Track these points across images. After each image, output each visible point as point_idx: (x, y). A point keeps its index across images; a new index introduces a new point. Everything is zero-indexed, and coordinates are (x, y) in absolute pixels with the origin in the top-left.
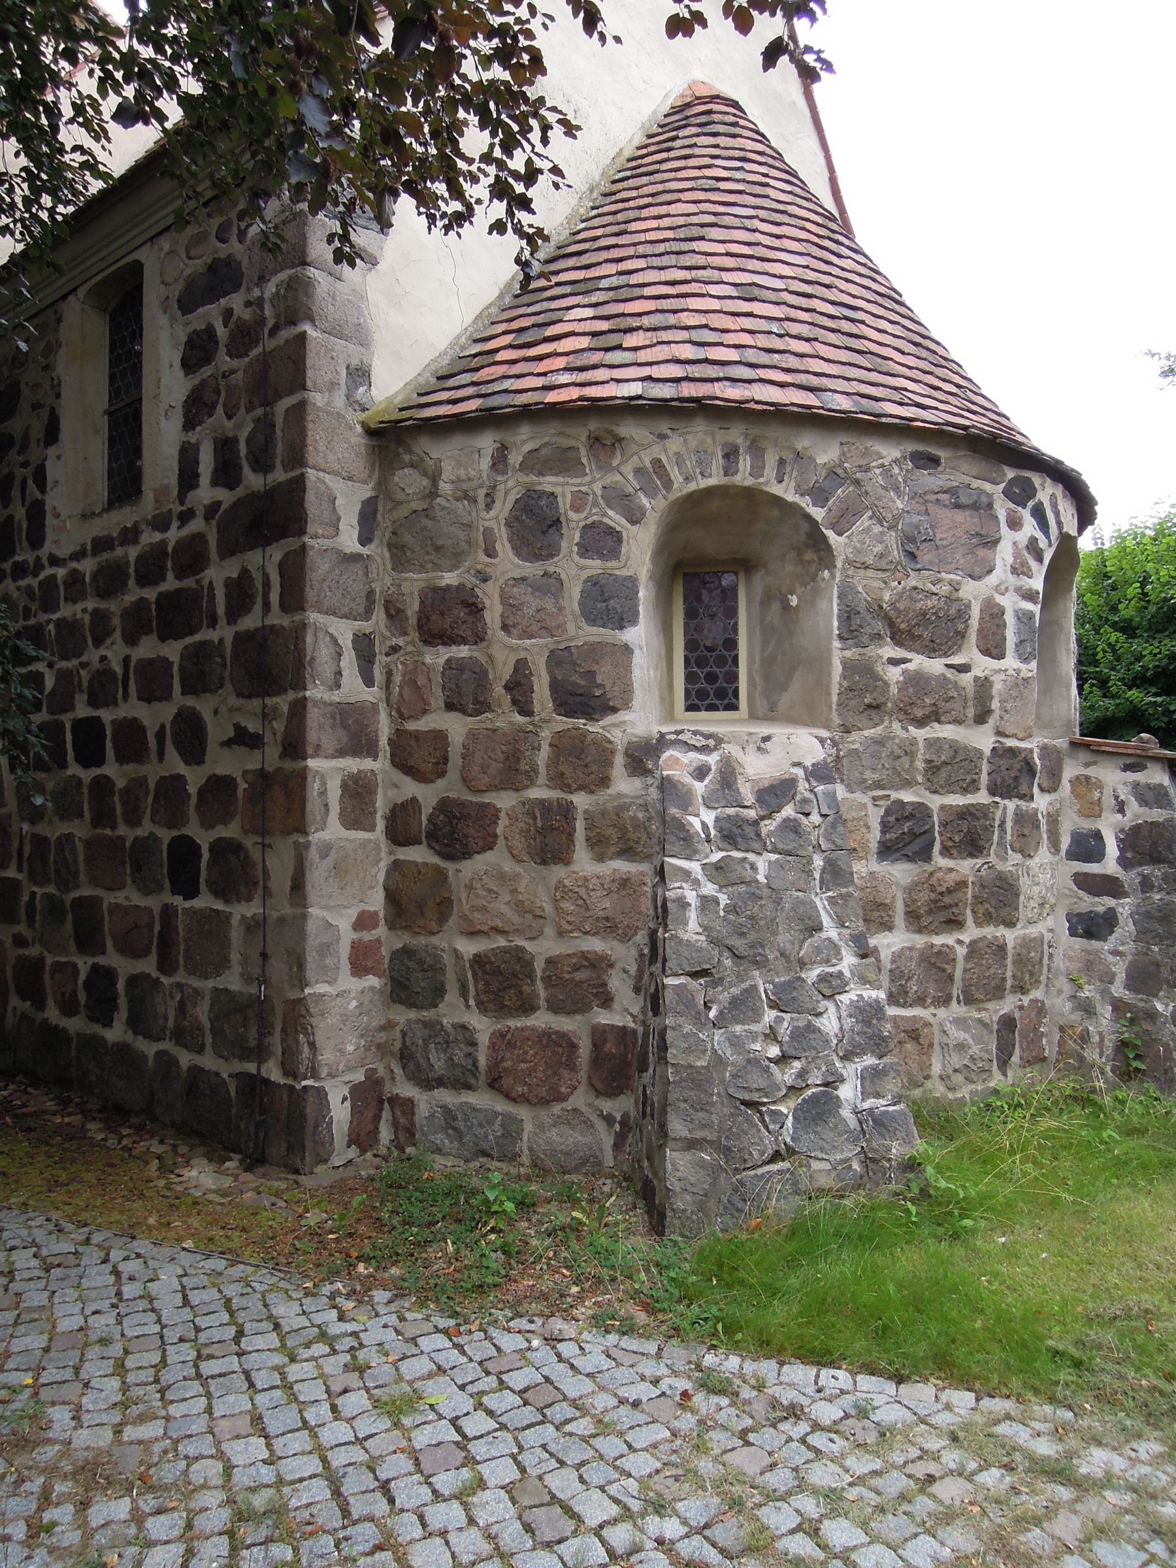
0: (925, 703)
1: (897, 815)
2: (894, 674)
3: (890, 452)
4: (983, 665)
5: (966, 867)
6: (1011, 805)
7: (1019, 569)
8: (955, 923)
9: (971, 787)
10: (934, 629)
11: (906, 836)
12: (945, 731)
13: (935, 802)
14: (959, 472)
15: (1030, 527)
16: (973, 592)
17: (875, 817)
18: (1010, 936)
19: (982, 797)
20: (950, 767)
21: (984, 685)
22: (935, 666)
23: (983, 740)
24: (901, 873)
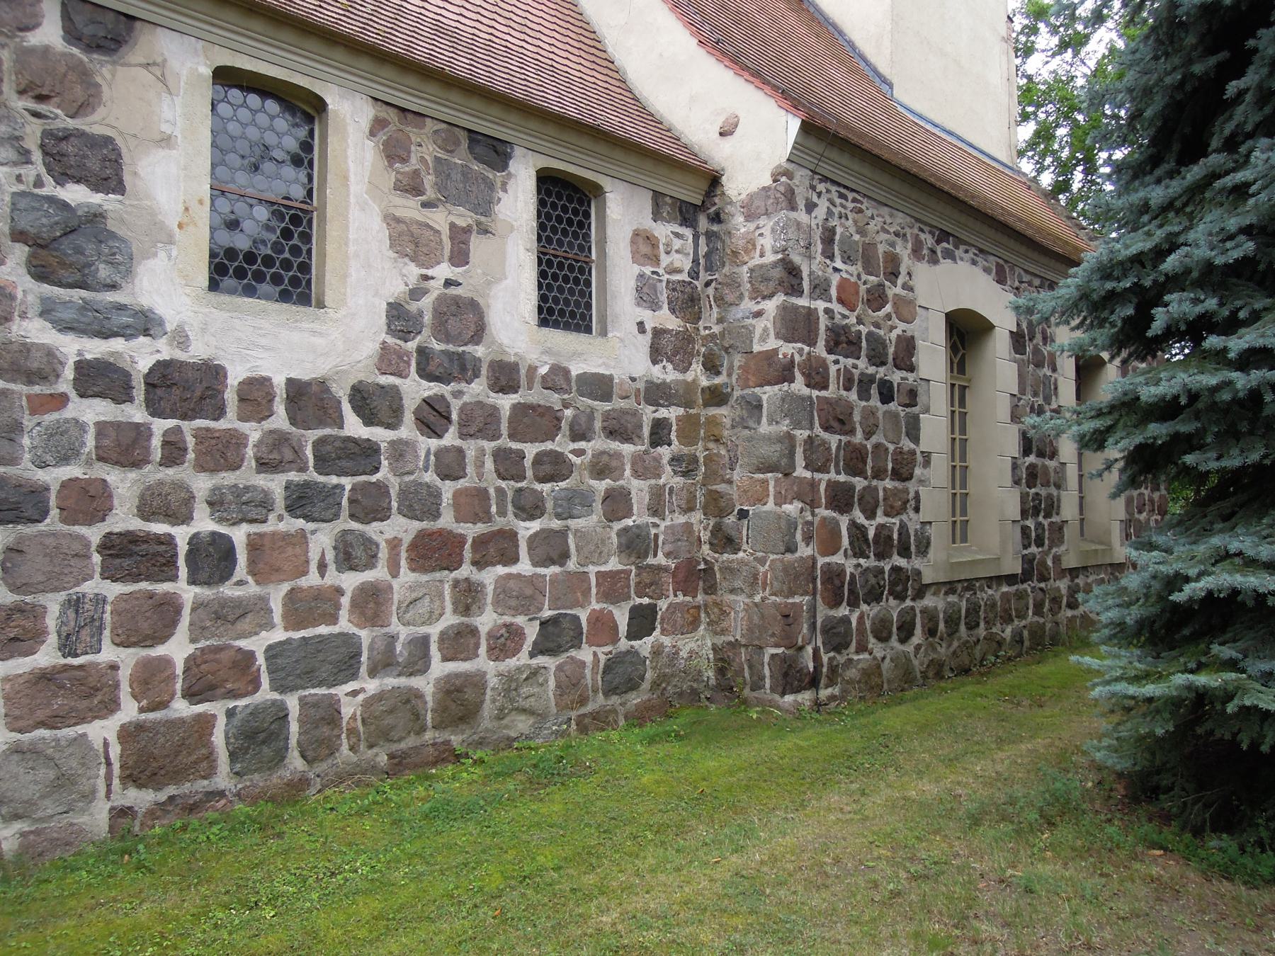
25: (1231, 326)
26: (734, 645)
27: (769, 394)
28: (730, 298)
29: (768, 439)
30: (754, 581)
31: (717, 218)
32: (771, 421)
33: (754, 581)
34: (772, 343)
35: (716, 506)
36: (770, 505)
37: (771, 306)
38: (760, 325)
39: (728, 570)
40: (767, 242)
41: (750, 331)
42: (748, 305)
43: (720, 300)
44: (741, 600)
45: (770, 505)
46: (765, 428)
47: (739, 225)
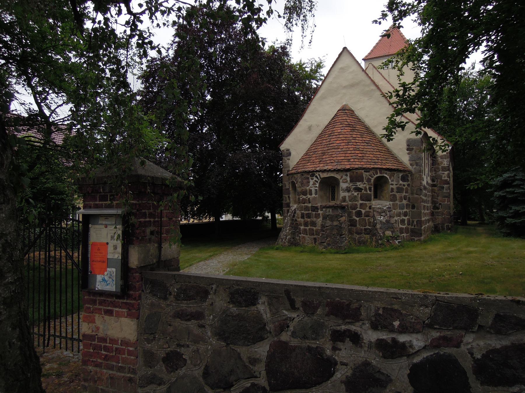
0: (304, 201)
1: (302, 214)
2: (301, 199)
3: (299, 175)
4: (309, 196)
5: (309, 220)
6: (314, 213)
7: (314, 184)
8: (308, 226)
9: (309, 211)
10: (305, 193)
11: (303, 217)
12: (306, 204)
13: (305, 212)
14: (305, 175)
15: (315, 179)
16: (308, 188)
17: (300, 214)
18: (314, 228)
19: (310, 212)
20: (307, 208)
21: (309, 199)
22: (304, 197)
23: (310, 205)
24: (302, 220)
25: (523, 185)
26: (439, 224)
27: (445, 186)
28: (437, 170)
29: (446, 193)
30: (443, 214)
31: (435, 157)
32: (446, 190)
33: (443, 214)
34: (446, 178)
35: (434, 202)
36: (446, 203)
37: (446, 173)
38: (444, 175)
39: (438, 212)
40: (445, 163)
41: (442, 176)
42: (441, 172)
43: (435, 171)
44: (440, 217)
45: (446, 203)
46: (445, 191)
47: (440, 160)
